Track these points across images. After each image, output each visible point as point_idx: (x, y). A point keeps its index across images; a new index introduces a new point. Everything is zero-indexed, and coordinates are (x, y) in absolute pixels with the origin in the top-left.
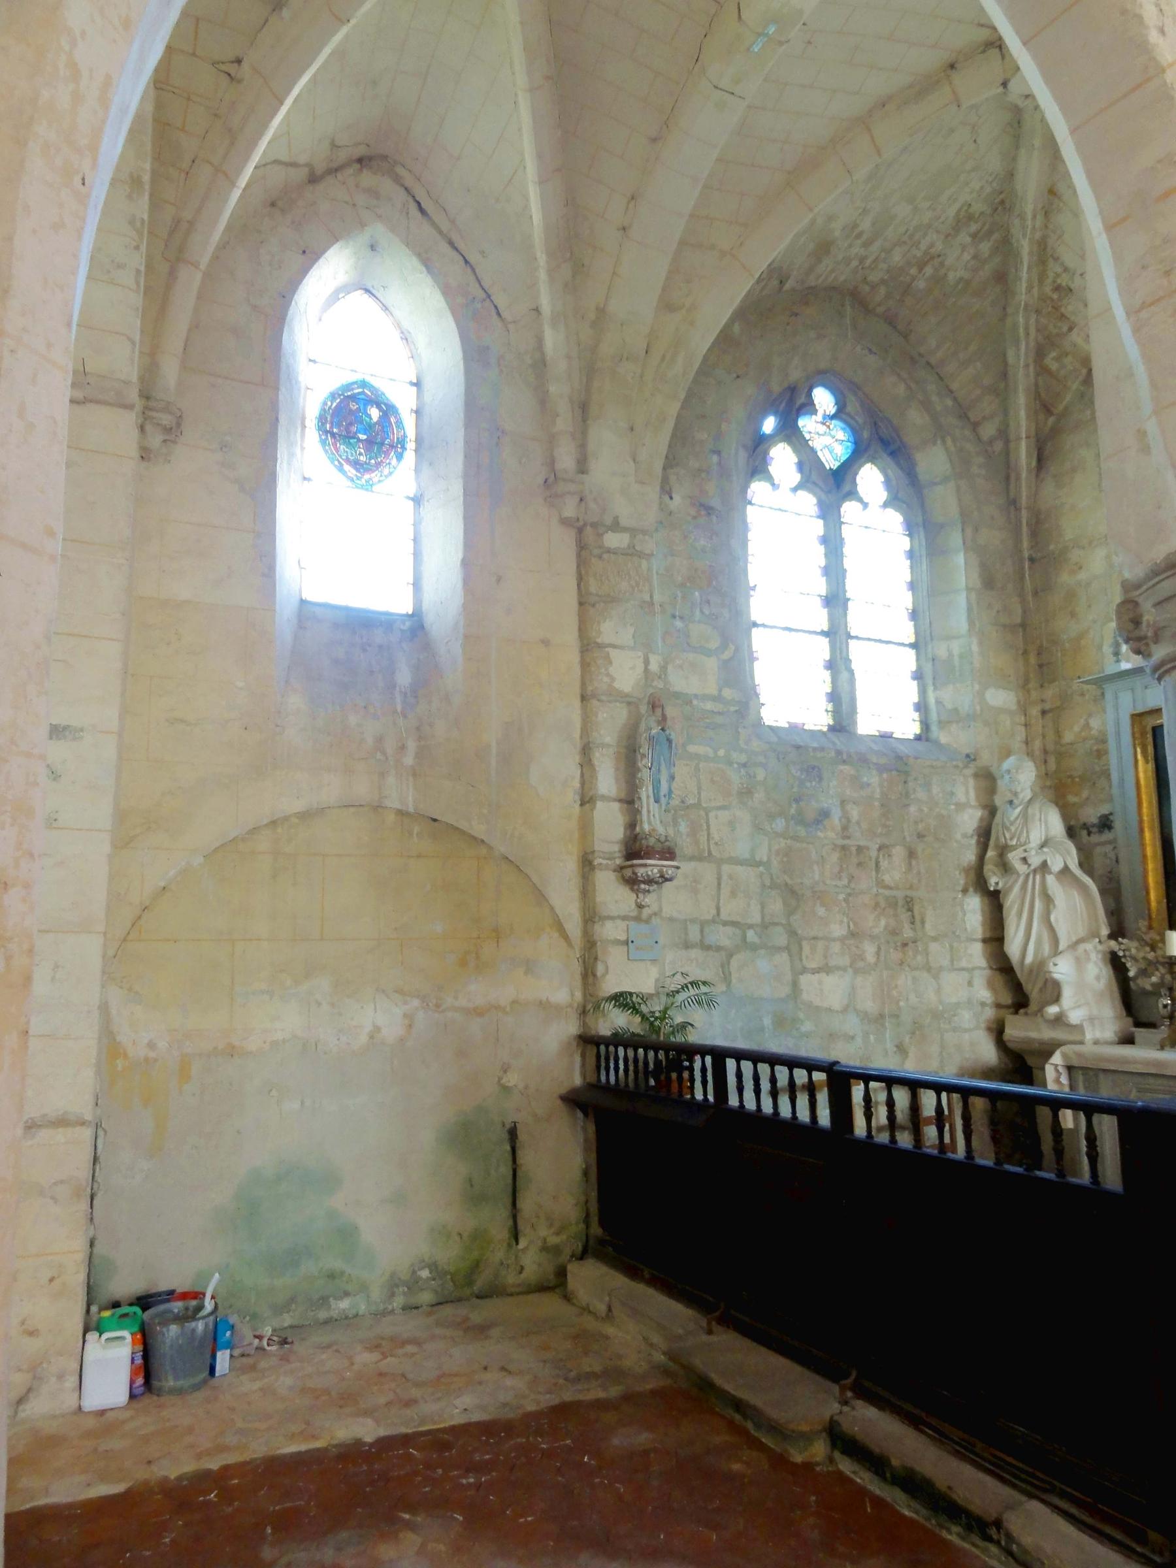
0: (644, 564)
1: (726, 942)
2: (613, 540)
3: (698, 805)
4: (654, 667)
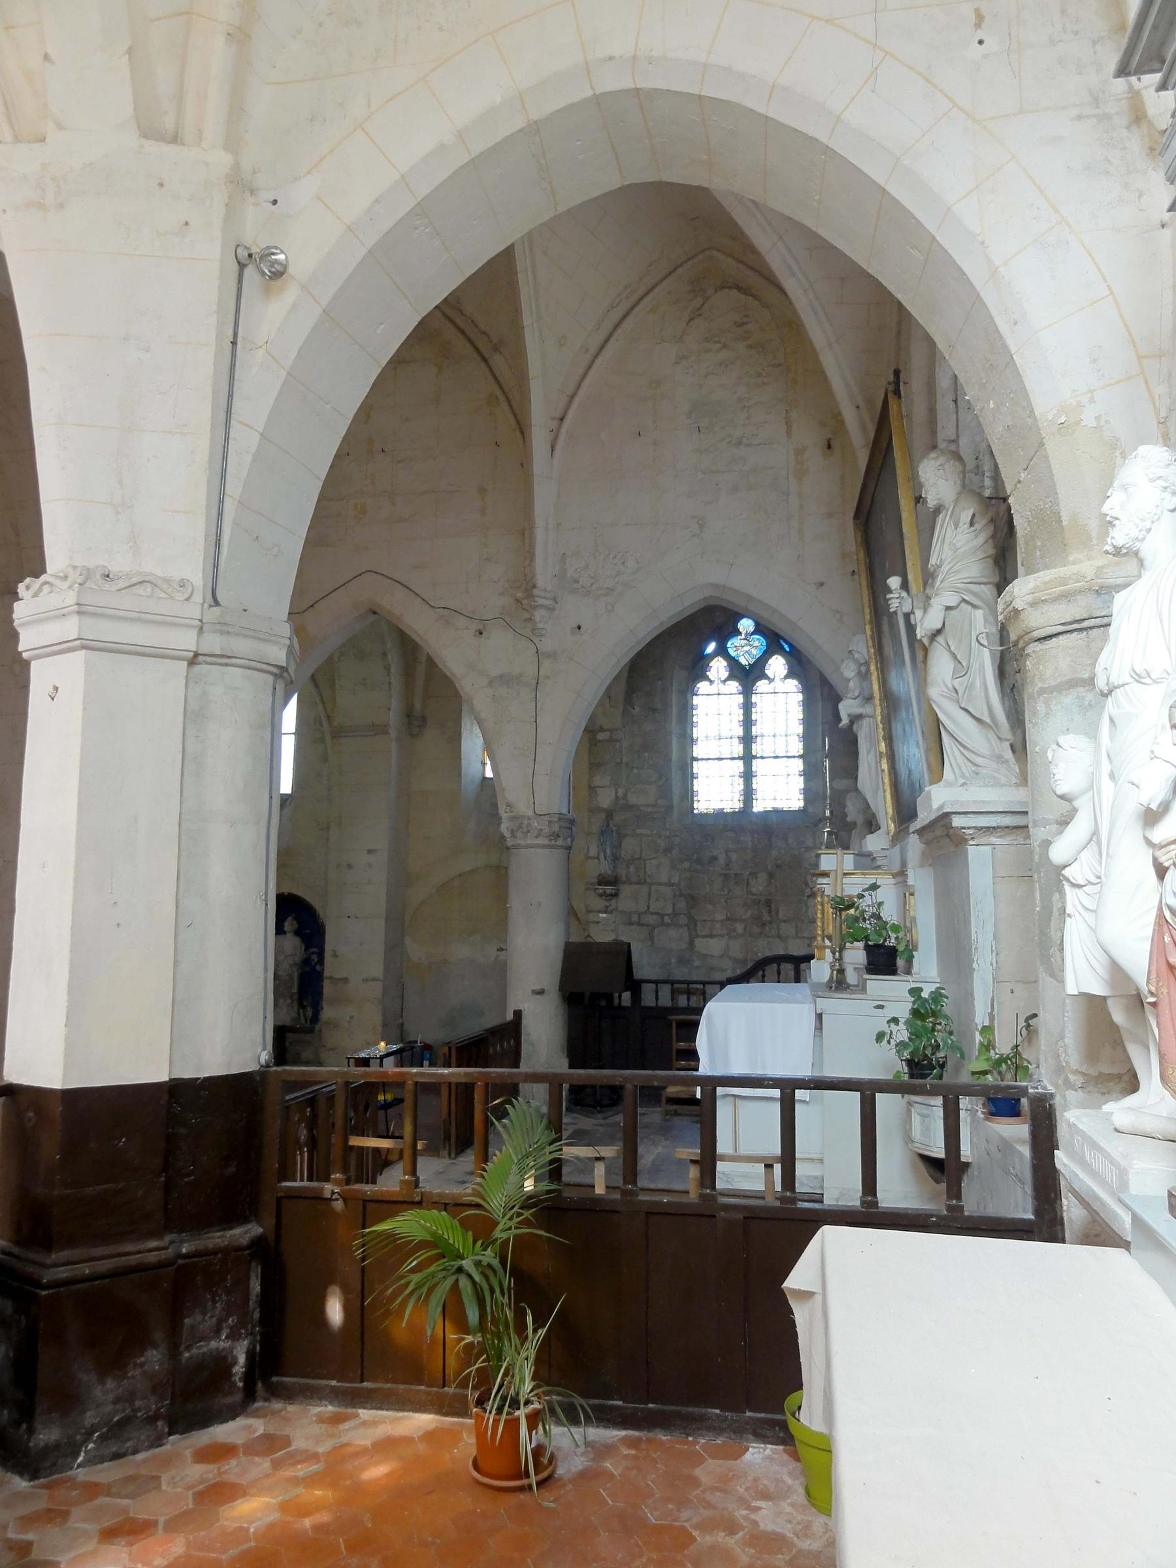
0: (618, 745)
1: (652, 922)
2: (601, 736)
3: (640, 859)
4: (620, 794)
